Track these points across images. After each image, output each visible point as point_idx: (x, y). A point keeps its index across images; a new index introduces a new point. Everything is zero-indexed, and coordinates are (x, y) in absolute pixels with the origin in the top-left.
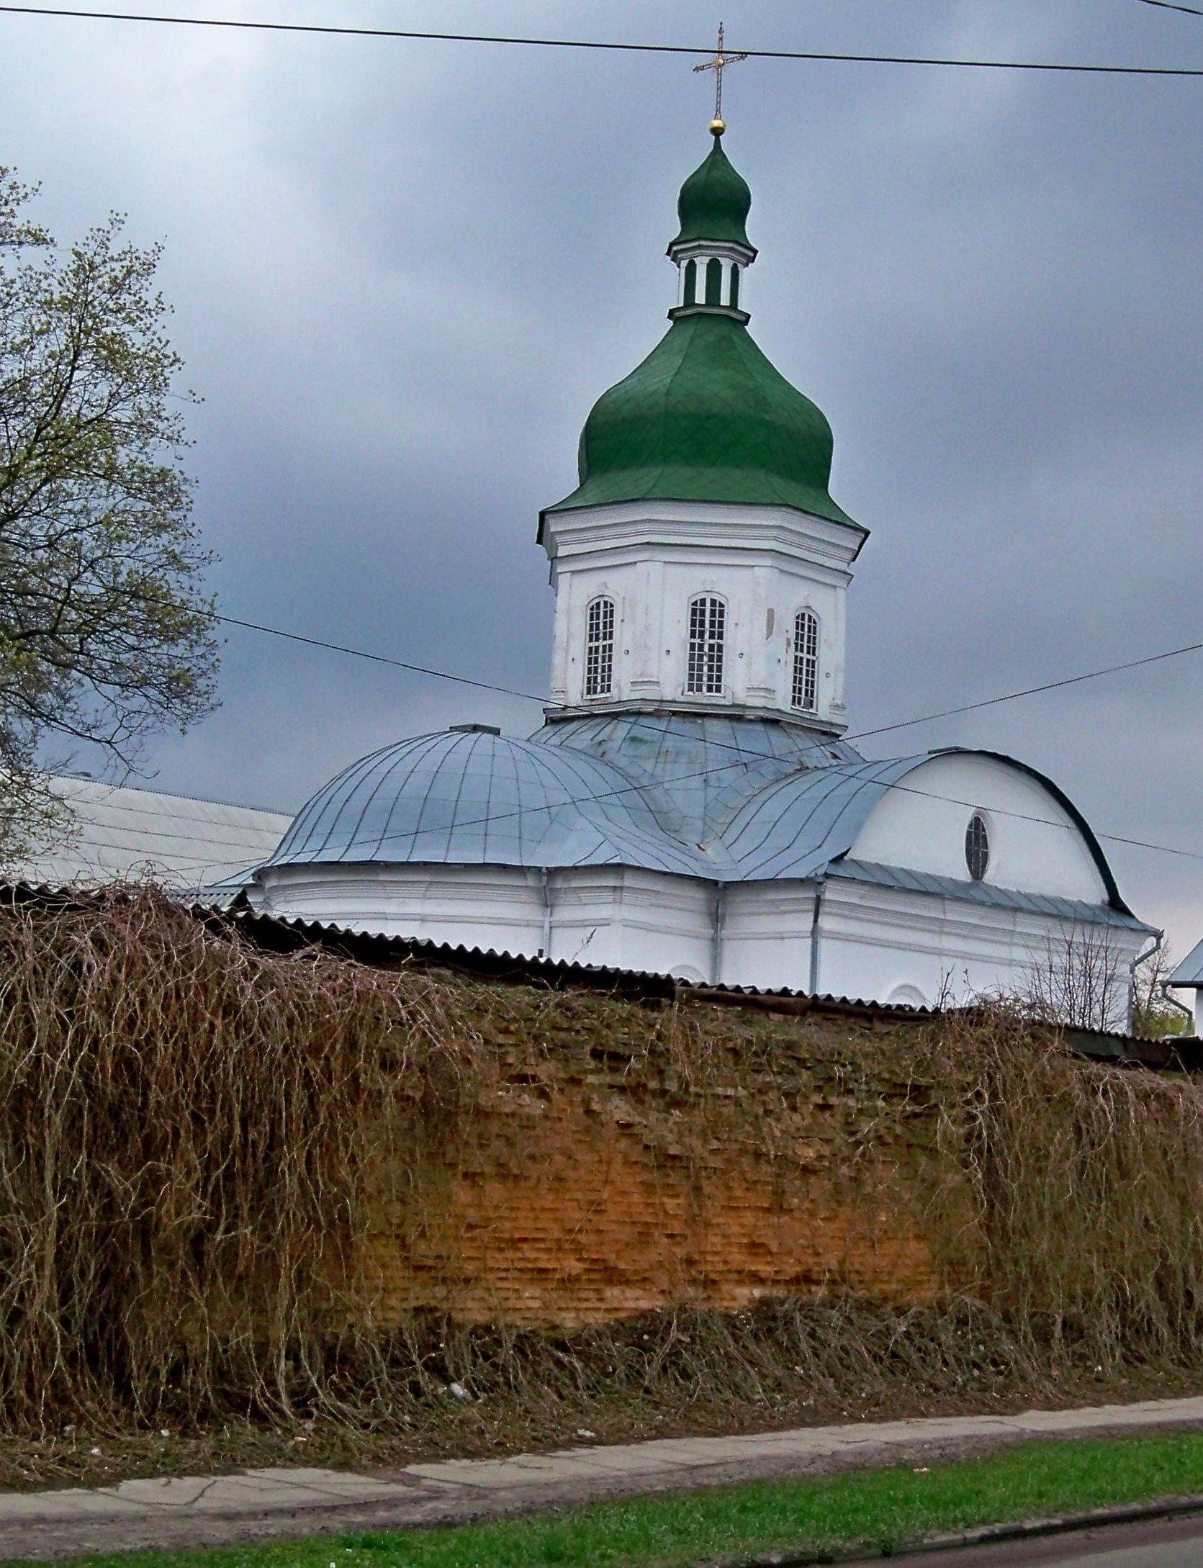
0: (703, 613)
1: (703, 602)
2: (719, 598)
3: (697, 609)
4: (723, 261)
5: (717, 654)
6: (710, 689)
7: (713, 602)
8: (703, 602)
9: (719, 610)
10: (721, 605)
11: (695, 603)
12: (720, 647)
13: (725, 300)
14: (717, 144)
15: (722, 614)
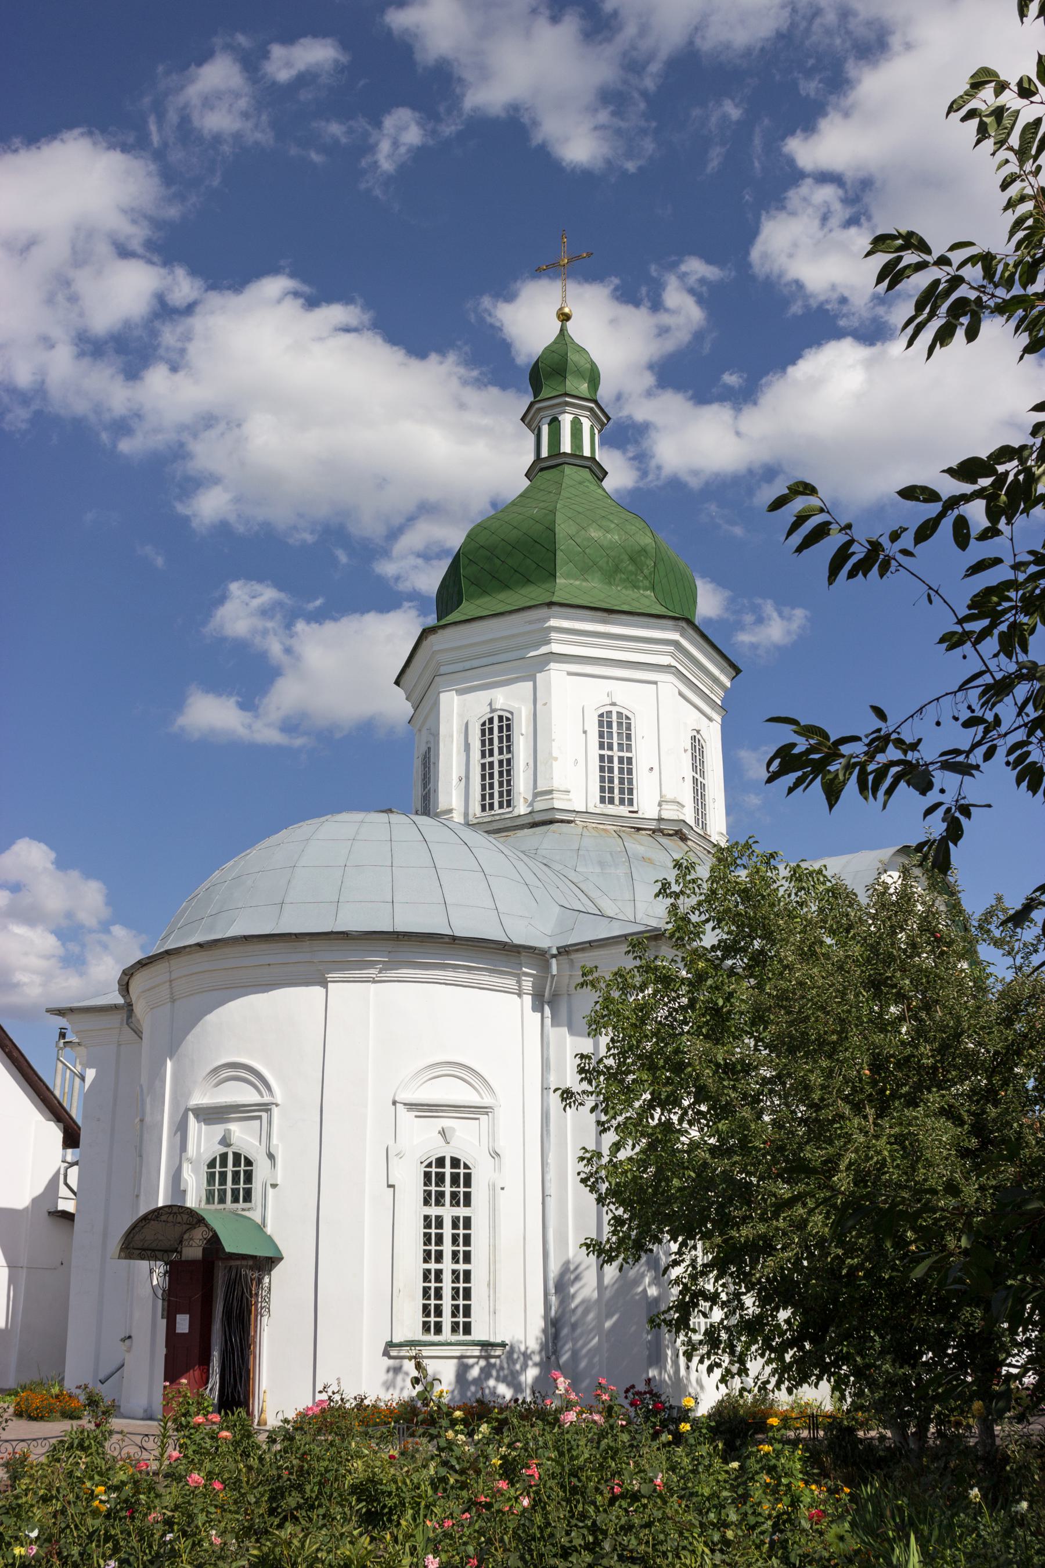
0: (491, 730)
1: (491, 720)
2: (505, 714)
3: (486, 729)
4: (583, 420)
5: (507, 767)
6: (501, 806)
7: (501, 718)
8: (491, 720)
9: (506, 725)
10: (508, 719)
11: (484, 724)
12: (630, 760)
13: (566, 447)
14: (563, 330)
15: (509, 727)
